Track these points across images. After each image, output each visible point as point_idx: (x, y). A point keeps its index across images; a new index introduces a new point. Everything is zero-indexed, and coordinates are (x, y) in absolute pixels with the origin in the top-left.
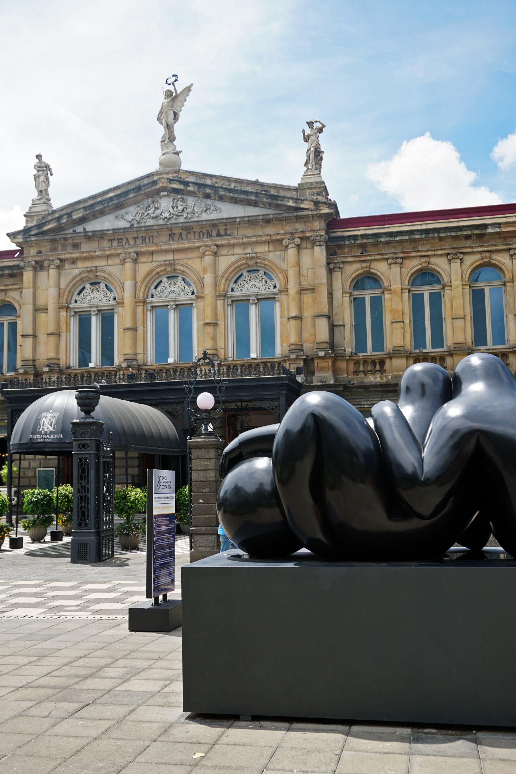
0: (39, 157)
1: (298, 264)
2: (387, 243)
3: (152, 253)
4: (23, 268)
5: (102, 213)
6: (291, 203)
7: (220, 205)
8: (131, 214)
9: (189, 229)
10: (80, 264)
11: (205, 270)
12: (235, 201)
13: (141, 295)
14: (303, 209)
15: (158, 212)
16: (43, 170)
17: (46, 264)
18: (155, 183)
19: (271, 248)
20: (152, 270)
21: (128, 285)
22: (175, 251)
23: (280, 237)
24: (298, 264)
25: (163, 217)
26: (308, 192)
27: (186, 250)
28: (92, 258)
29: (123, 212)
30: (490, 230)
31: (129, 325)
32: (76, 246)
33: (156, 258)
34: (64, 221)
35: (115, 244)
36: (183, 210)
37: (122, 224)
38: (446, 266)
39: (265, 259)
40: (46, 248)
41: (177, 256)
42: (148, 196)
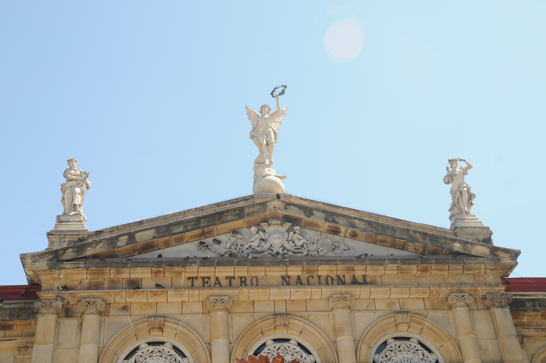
1: (473, 330)
11: (337, 331)
16: (73, 182)
24: (473, 330)
25: (275, 252)
36: (302, 246)
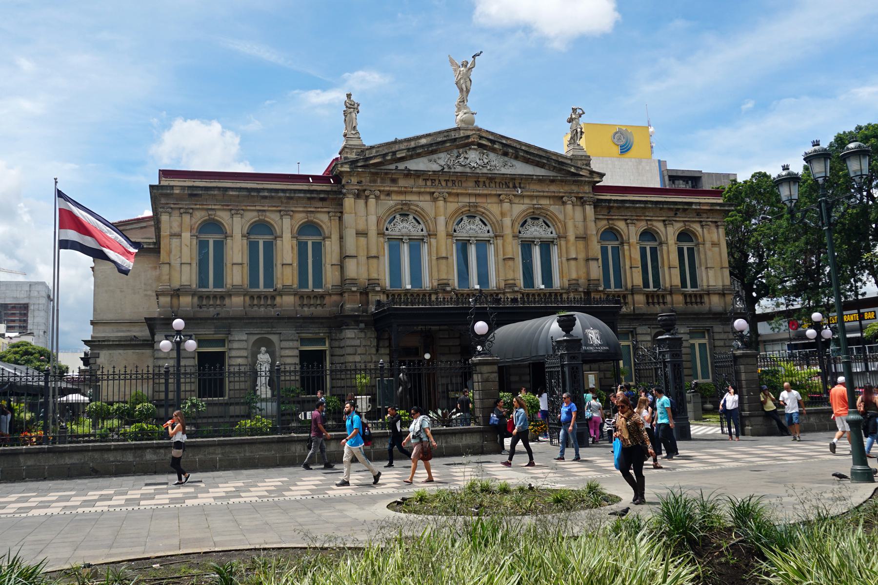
0: (349, 96)
2: (619, 208)
3: (458, 195)
4: (344, 194)
5: (419, 155)
6: (573, 170)
7: (515, 162)
8: (442, 160)
9: (492, 179)
10: (394, 197)
11: (503, 214)
12: (527, 161)
13: (450, 230)
14: (582, 176)
15: (468, 161)
17: (367, 193)
18: (468, 137)
19: (552, 202)
20: (460, 209)
21: (441, 220)
22: (476, 195)
23: (561, 195)
26: (579, 162)
27: (486, 195)
28: (405, 193)
29: (435, 156)
30: (694, 207)
31: (444, 255)
32: (394, 181)
33: (461, 199)
34: (389, 158)
35: (429, 183)
37: (435, 167)
38: (663, 229)
39: (548, 210)
40: (366, 180)
41: (479, 200)
42: (458, 147)
